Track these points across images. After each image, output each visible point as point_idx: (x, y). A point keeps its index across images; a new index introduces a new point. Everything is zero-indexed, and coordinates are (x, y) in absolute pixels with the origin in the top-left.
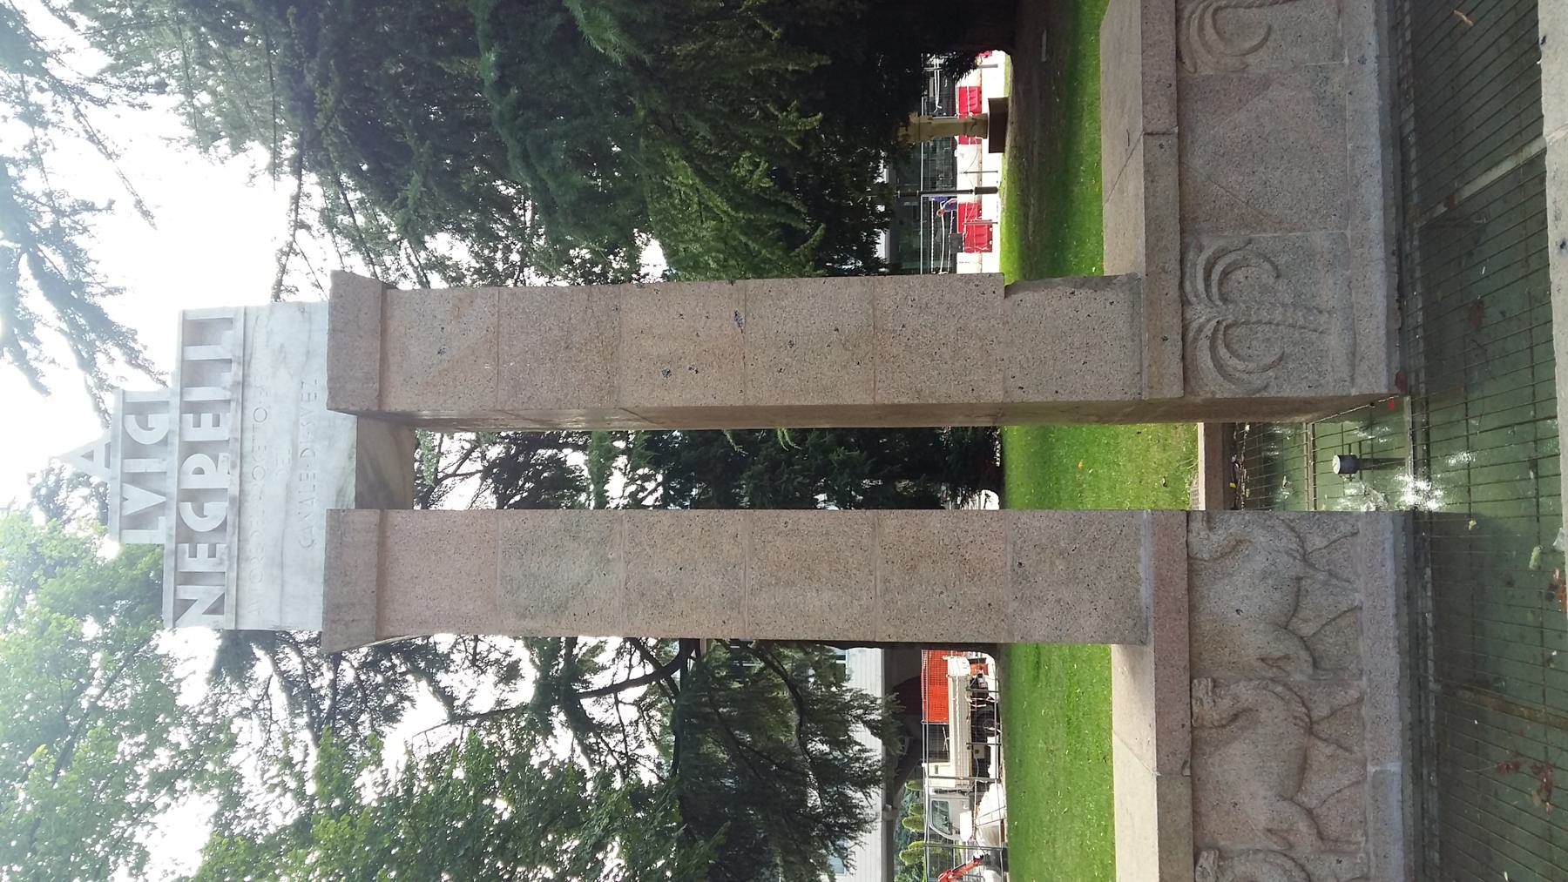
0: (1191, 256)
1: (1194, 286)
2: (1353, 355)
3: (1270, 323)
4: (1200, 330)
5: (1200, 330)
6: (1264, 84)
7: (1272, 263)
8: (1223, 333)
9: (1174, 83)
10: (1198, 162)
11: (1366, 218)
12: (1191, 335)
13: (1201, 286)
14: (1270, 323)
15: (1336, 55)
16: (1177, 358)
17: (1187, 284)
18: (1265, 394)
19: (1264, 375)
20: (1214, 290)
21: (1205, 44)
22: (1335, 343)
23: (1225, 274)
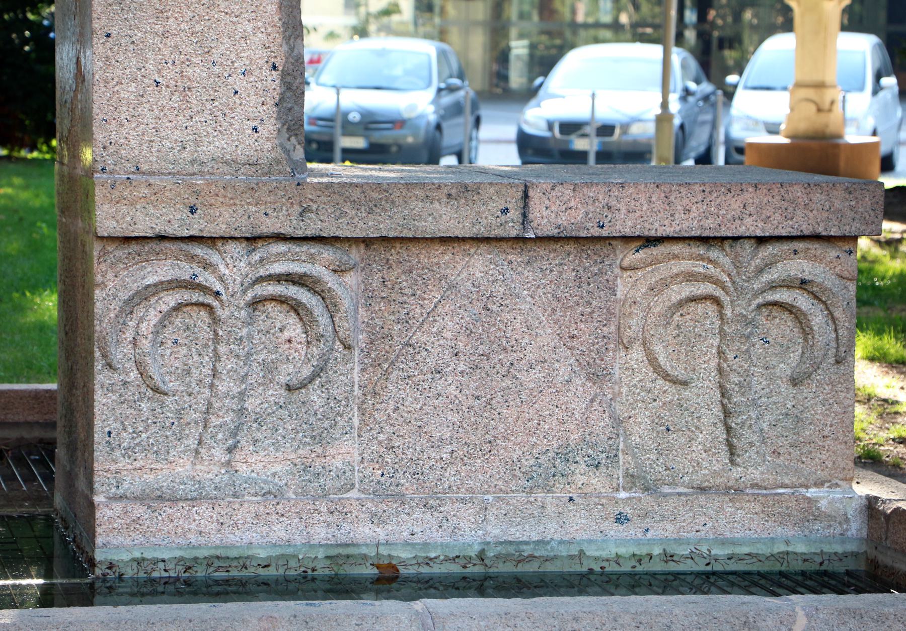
0: (327, 254)
1: (279, 257)
2: (155, 498)
3: (215, 374)
4: (206, 265)
5: (206, 265)
6: (598, 375)
7: (311, 379)
8: (202, 299)
9: (605, 233)
10: (478, 266)
11: (375, 518)
12: (199, 250)
13: (278, 268)
14: (215, 374)
15: (632, 480)
16: (161, 228)
17: (281, 247)
18: (98, 366)
19: (130, 365)
20: (272, 289)
21: (665, 284)
22: (181, 468)
23: (296, 307)
